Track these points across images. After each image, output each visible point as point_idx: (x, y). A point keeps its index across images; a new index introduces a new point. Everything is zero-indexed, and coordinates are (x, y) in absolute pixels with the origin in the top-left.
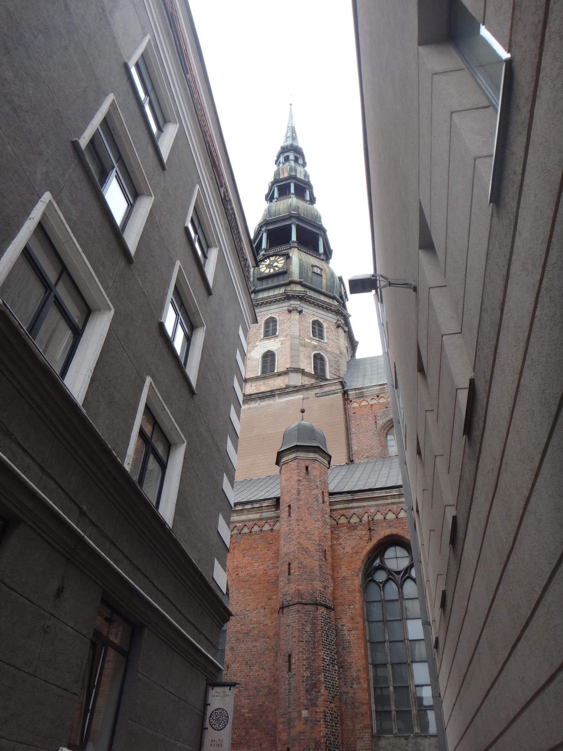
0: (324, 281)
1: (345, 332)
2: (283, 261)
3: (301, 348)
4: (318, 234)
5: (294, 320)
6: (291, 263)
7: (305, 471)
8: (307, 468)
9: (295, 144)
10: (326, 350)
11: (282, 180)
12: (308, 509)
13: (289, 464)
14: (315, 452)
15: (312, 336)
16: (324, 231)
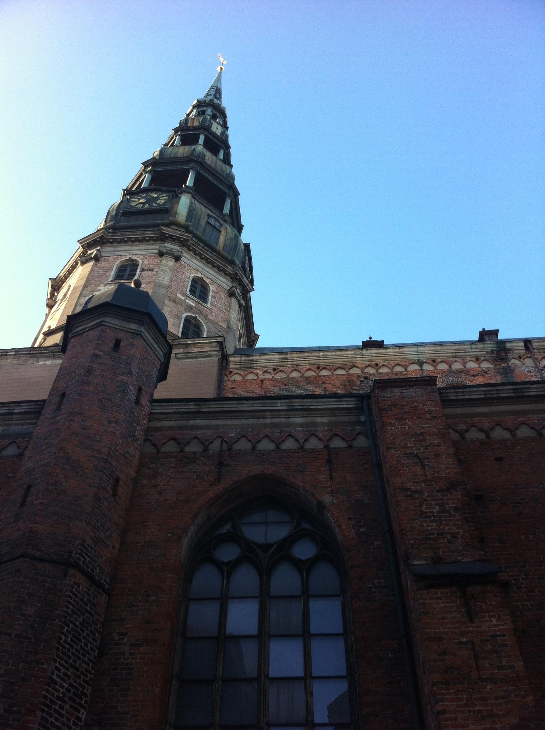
0: (222, 239)
1: (240, 306)
2: (167, 198)
3: (167, 302)
4: (225, 193)
5: (166, 265)
6: (178, 203)
7: (112, 345)
8: (117, 343)
9: (216, 101)
10: (206, 317)
11: (189, 129)
12: (101, 400)
13: (85, 335)
14: (141, 323)
15: (188, 293)
16: (236, 194)
